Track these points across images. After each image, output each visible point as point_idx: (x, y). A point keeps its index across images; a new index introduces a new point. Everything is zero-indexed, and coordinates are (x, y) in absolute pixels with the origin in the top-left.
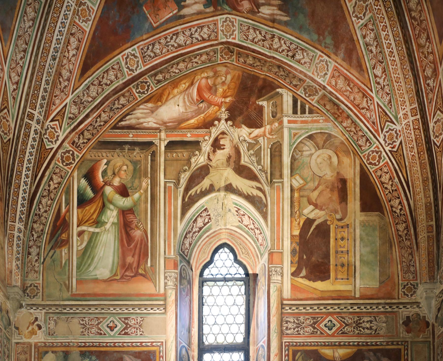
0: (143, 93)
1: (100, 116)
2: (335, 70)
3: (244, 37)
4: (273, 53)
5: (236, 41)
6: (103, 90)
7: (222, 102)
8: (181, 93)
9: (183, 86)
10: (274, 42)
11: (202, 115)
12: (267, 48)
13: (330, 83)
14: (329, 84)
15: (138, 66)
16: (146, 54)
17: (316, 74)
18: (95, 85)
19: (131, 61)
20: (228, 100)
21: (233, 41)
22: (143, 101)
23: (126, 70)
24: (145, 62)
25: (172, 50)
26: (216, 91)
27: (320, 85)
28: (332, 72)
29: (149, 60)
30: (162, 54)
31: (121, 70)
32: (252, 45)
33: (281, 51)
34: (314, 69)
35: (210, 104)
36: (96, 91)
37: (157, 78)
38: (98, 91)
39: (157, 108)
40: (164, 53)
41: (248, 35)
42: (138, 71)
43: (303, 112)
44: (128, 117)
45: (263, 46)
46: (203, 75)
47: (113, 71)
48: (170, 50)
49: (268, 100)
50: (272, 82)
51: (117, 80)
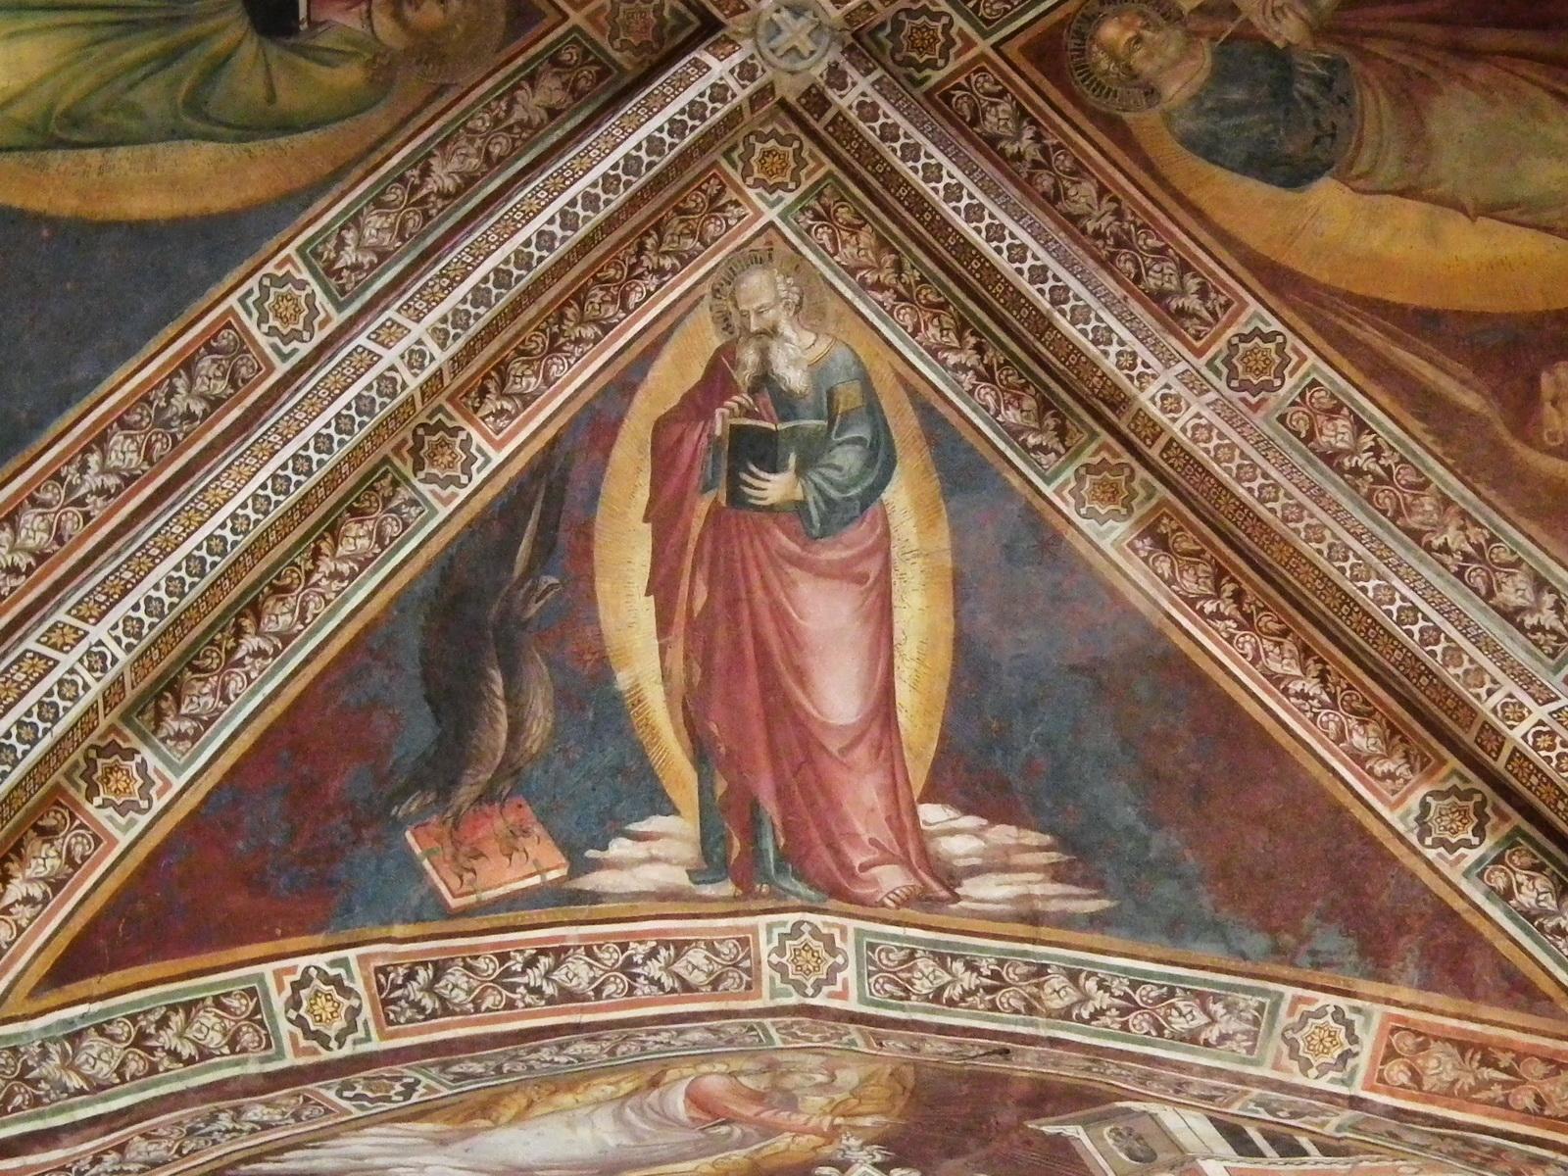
0: (388, 1099)
1: (121, 1148)
2: (1396, 1030)
3: (887, 987)
4: (1053, 1027)
5: (853, 1005)
6: (153, 1069)
7: (834, 1128)
8: (598, 1103)
9: (603, 1089)
10: (1048, 990)
11: (743, 1152)
12: (1017, 1011)
13: (1381, 1080)
14: (1381, 1082)
15: (352, 1027)
16: (398, 993)
17: (1295, 1066)
18: (112, 1037)
19: (322, 1001)
20: (867, 1122)
21: (836, 1004)
22: (384, 1117)
23: (285, 1027)
24: (390, 1023)
25: (528, 1006)
26: (791, 1102)
27: (1332, 1098)
28: (1377, 1041)
29: (409, 1021)
30: (477, 1010)
31: (261, 1023)
32: (933, 1012)
33: (1086, 1015)
34: (1279, 1052)
35: (770, 1131)
36: (115, 1064)
37: (456, 1069)
38: (123, 1064)
39: (472, 1133)
40: (488, 1010)
41: (909, 981)
42: (347, 1050)
43: (1289, 1148)
44: (287, 1155)
45: (995, 1008)
46: (705, 1068)
47: (216, 1015)
48: (521, 1004)
49: (1085, 1123)
50: (1082, 1087)
51: (233, 1052)
